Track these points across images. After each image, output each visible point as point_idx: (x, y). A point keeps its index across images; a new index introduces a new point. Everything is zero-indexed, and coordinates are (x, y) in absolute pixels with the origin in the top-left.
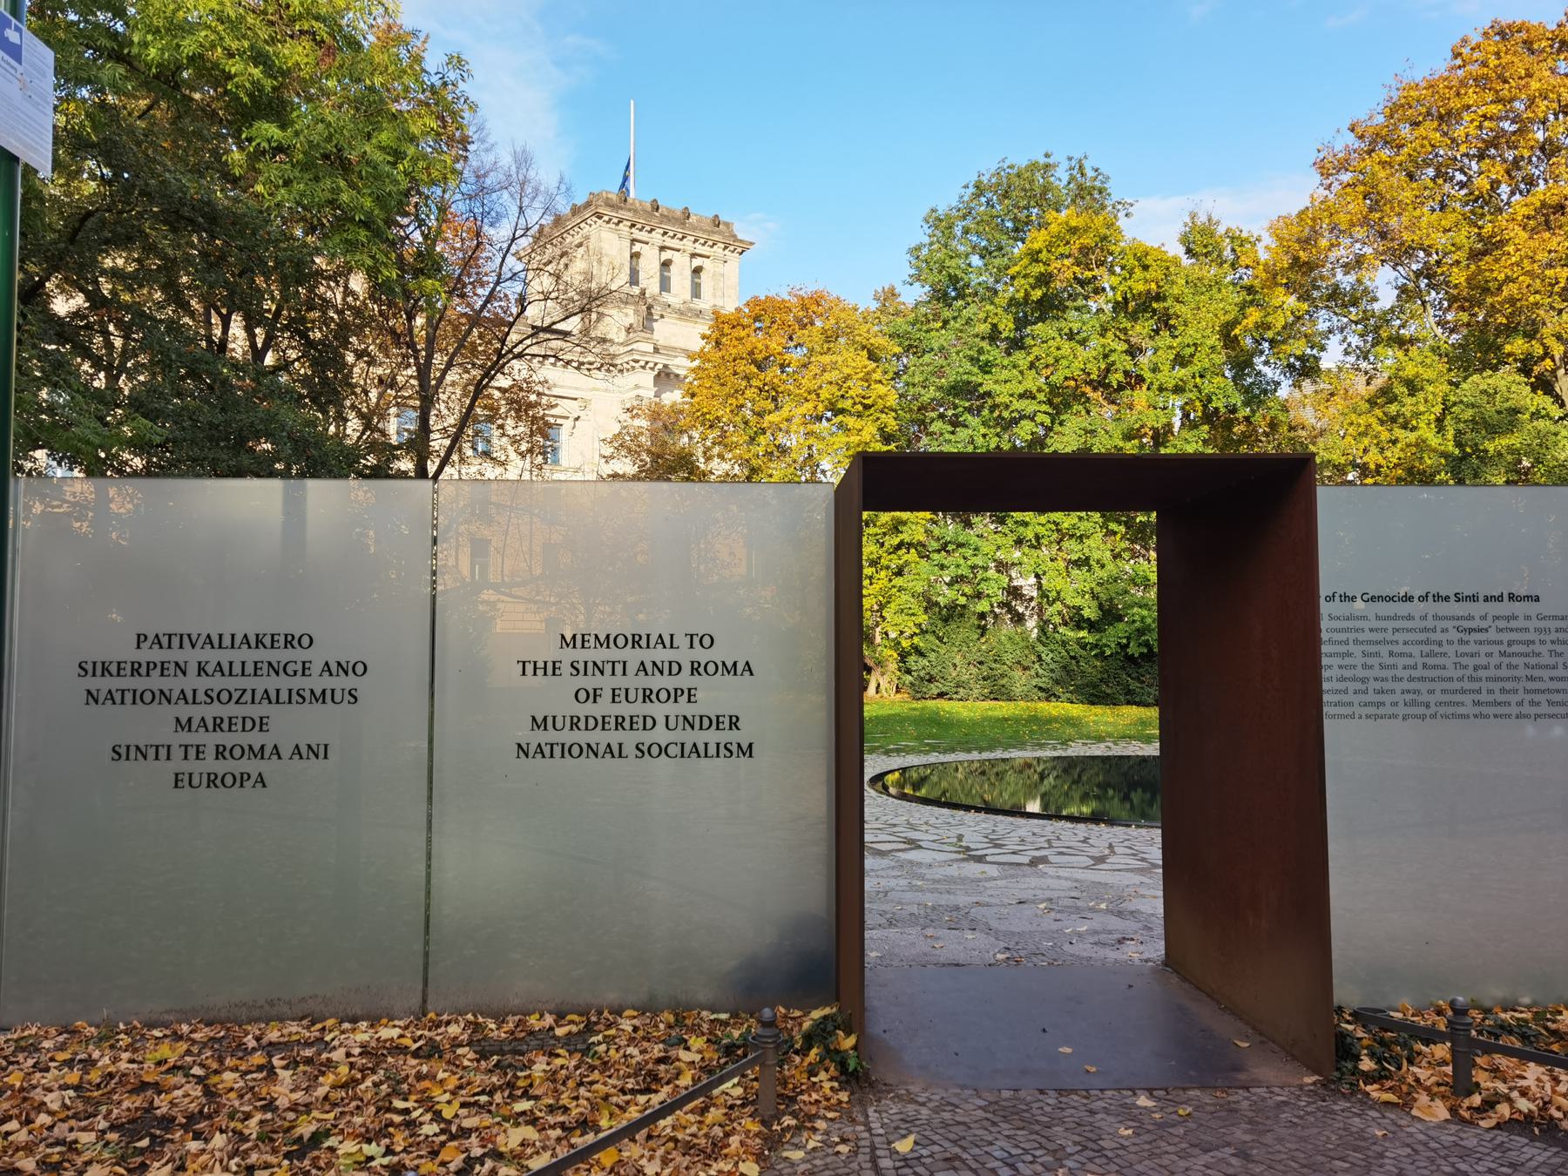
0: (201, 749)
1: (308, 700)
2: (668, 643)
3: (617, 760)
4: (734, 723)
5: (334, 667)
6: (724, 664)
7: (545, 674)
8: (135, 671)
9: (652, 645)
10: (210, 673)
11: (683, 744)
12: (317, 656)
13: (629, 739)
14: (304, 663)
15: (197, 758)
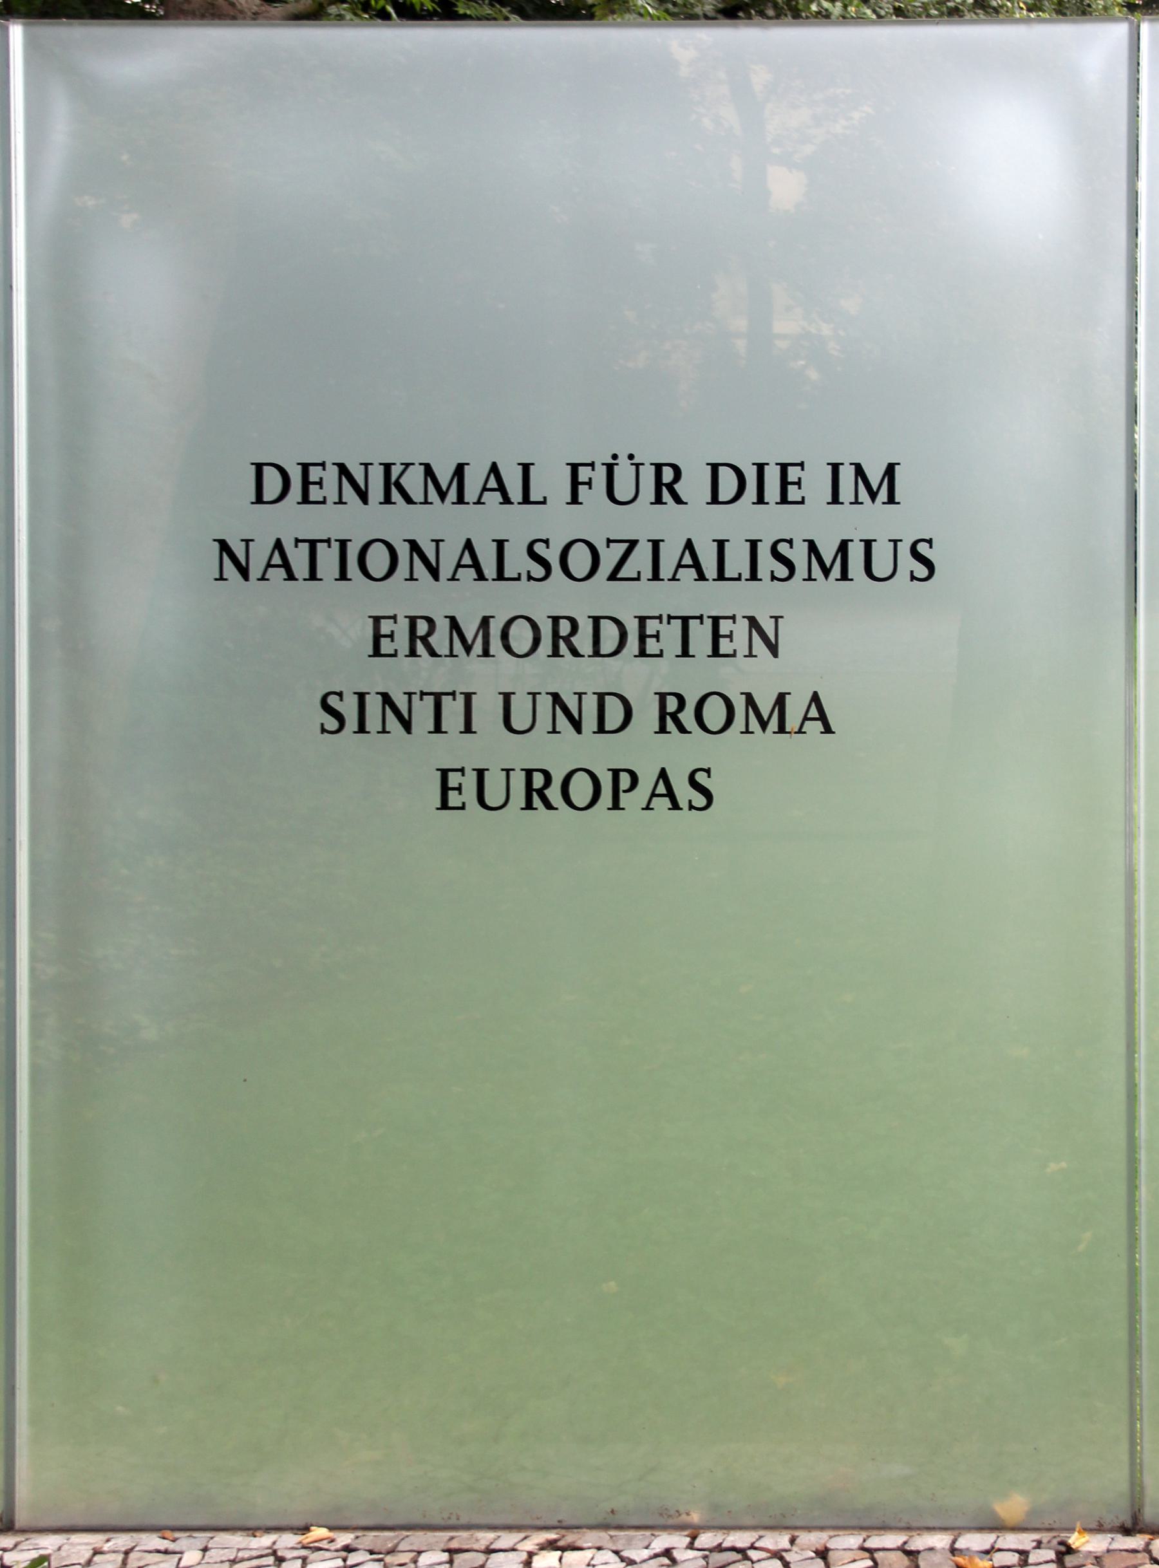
6: (750, 700)
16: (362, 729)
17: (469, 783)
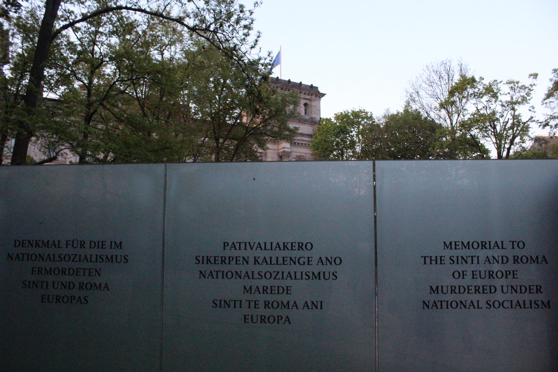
0: (257, 303)
1: (311, 278)
3: (477, 310)
5: (324, 260)
6: (531, 257)
7: (436, 263)
8: (223, 261)
10: (261, 263)
11: (511, 301)
12: (315, 255)
13: (482, 298)
14: (308, 258)
15: (255, 307)
16: (458, 263)
17: (478, 273)
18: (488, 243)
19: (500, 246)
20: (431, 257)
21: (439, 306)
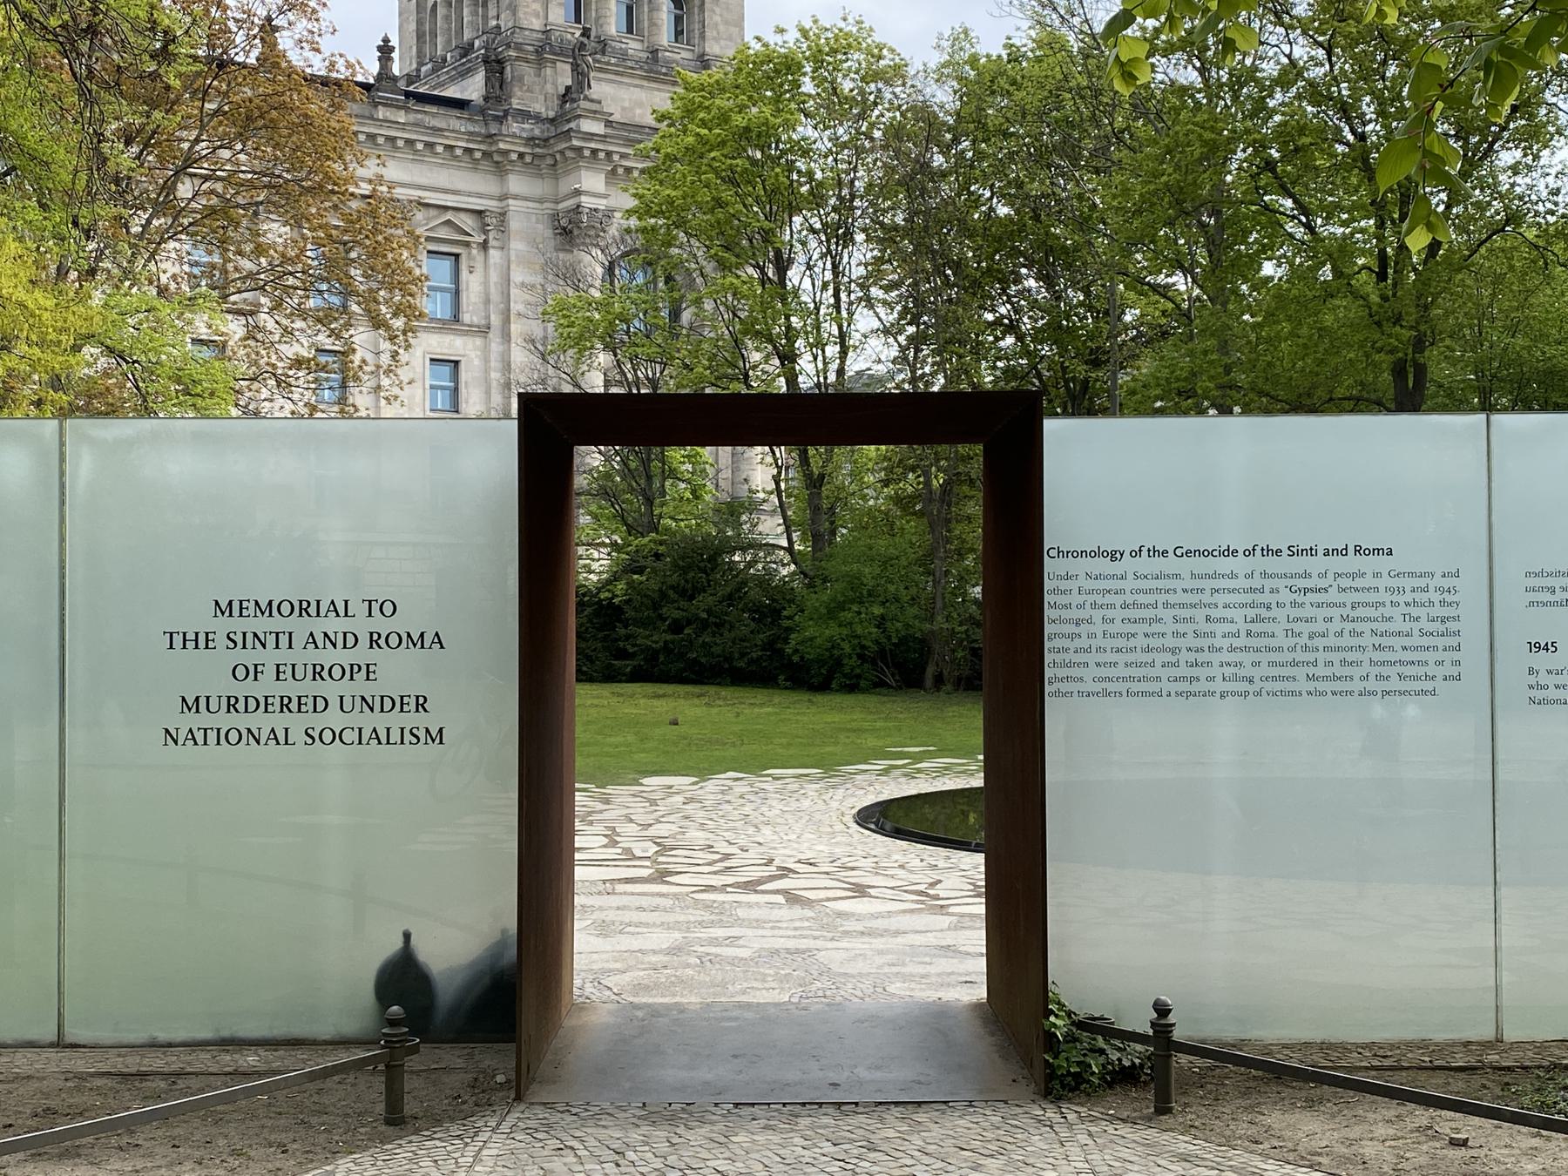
2: (342, 612)
4: (421, 705)
6: (409, 635)
7: (197, 647)
9: (322, 613)
11: (360, 729)
13: (296, 723)
16: (244, 647)
18: (314, 604)
19: (341, 611)
20: (184, 634)
21: (200, 739)
